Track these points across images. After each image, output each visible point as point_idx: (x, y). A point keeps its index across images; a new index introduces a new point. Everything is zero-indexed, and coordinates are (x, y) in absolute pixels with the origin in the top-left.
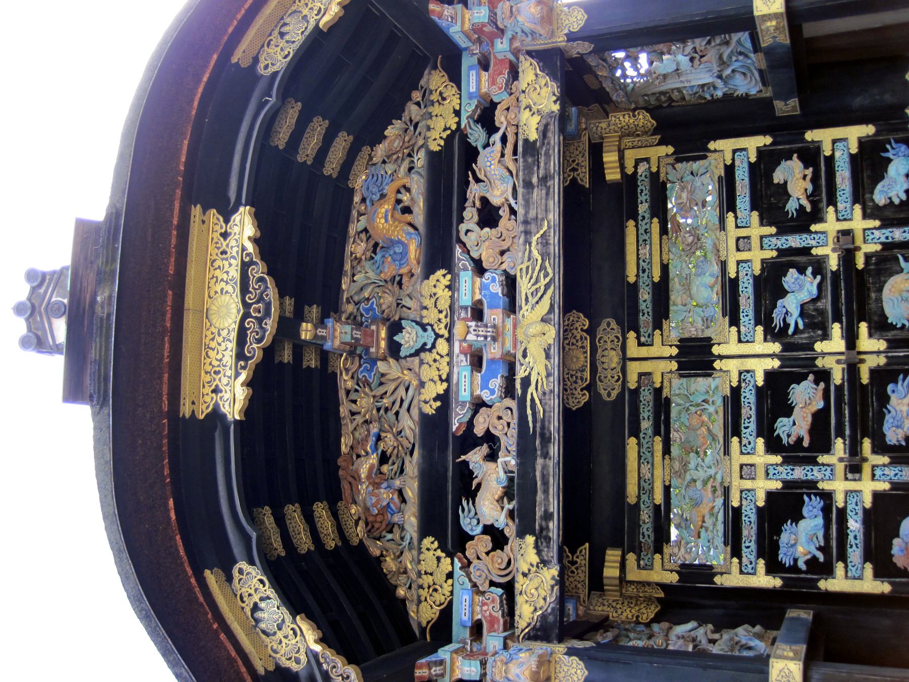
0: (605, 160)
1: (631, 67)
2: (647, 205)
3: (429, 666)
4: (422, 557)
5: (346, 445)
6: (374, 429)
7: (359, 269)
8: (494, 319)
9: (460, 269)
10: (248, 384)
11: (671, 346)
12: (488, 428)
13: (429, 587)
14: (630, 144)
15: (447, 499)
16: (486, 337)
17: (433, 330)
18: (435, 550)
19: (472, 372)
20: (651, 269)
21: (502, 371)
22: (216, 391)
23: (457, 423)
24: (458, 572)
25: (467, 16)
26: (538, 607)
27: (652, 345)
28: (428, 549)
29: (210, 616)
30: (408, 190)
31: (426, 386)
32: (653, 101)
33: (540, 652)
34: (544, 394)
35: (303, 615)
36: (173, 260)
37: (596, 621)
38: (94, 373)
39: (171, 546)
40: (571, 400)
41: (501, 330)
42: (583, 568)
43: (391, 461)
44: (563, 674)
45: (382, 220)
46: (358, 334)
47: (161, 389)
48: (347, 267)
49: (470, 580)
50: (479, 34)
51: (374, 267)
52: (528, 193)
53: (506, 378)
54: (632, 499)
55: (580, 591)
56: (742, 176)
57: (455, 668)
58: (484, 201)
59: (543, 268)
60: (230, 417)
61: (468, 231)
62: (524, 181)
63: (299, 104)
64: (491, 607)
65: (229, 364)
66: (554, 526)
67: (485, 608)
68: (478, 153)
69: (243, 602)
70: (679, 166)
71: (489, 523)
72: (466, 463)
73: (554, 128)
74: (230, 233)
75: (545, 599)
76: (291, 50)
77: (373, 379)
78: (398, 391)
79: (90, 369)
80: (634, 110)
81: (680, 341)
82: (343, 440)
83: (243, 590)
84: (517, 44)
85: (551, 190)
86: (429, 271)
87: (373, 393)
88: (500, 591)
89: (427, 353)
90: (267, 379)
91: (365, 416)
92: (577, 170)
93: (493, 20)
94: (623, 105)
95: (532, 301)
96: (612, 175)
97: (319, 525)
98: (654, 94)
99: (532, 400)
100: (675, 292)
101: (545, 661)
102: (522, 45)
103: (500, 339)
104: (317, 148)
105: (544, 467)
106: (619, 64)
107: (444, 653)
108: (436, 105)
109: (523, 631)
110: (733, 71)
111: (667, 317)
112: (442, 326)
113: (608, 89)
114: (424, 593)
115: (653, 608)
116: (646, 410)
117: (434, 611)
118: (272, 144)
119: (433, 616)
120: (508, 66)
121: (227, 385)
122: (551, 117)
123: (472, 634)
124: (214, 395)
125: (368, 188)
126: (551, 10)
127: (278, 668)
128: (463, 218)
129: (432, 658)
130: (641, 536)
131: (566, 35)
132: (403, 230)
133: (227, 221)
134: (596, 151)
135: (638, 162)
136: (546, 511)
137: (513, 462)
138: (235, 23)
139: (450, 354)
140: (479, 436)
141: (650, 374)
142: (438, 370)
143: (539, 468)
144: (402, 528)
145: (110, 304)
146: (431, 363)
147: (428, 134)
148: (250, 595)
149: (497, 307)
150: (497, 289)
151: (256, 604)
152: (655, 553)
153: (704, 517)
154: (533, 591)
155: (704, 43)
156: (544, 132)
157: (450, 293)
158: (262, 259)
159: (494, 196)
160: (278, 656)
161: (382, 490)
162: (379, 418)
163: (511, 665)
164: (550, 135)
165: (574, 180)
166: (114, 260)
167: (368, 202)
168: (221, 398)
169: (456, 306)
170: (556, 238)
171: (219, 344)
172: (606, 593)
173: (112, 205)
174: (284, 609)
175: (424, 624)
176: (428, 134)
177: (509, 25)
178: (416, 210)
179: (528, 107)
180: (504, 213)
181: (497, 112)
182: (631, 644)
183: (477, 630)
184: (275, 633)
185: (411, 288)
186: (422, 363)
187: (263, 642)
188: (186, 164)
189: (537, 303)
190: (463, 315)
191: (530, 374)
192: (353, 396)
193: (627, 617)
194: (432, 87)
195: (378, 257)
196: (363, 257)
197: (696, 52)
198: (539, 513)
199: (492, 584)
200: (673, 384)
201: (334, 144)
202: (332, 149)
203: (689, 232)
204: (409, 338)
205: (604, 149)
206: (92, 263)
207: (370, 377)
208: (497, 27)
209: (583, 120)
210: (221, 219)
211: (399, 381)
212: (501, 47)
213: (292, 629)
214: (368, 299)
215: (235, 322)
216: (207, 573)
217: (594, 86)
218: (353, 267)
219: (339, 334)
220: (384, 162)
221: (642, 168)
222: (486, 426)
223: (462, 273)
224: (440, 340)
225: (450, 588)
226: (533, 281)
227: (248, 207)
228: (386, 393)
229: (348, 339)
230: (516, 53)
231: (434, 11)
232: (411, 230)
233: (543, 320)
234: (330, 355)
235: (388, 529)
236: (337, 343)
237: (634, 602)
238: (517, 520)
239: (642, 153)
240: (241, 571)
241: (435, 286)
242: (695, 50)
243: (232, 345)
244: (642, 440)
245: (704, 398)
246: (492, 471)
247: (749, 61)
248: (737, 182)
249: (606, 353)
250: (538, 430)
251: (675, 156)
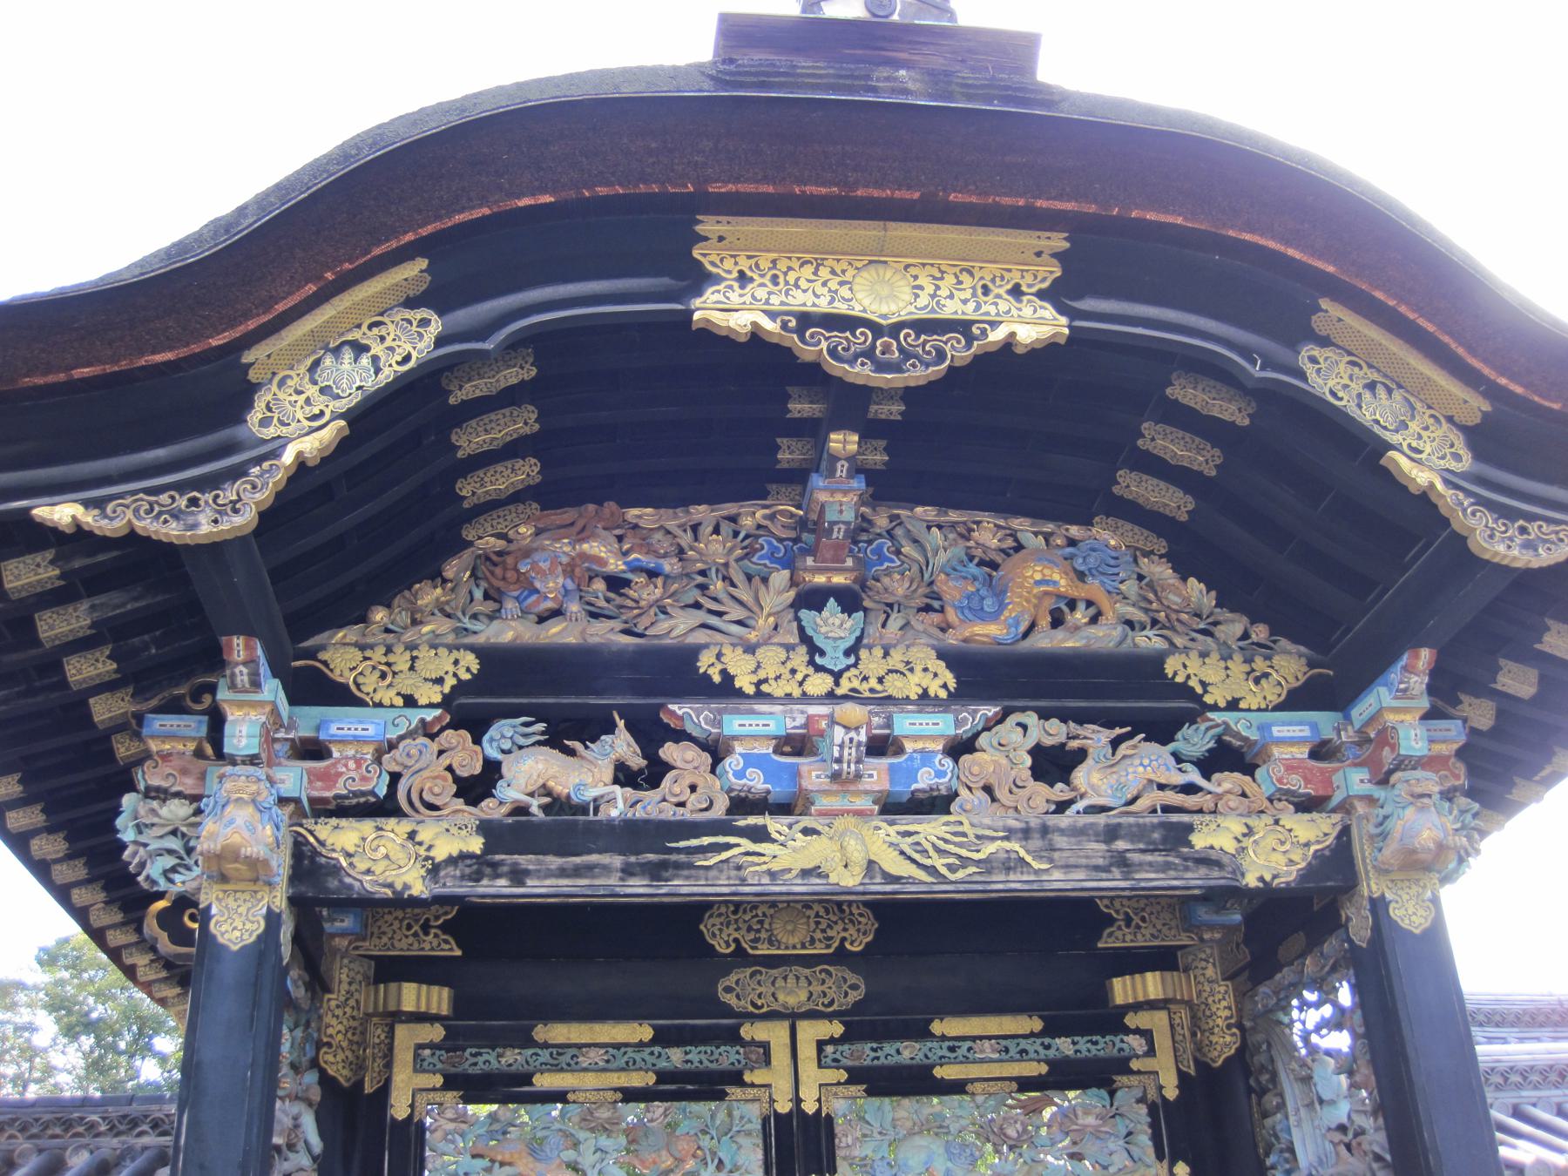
0: (1149, 975)
1: (1323, 1018)
2: (1071, 1053)
3: (251, 662)
4: (443, 651)
5: (640, 517)
6: (669, 566)
7: (951, 536)
8: (871, 776)
9: (956, 714)
10: (756, 336)
11: (819, 1100)
12: (674, 768)
13: (389, 664)
14: (1178, 1021)
15: (547, 695)
16: (839, 761)
17: (848, 668)
18: (455, 675)
19: (775, 738)
20: (956, 1061)
21: (778, 792)
22: (743, 279)
23: (684, 711)
24: (416, 716)
25: (1408, 717)
26: (355, 860)
27: (820, 1066)
28: (456, 662)
29: (347, 266)
30: (1094, 620)
31: (748, 657)
32: (1261, 1059)
33: (274, 864)
34: (739, 868)
35: (347, 432)
36: (974, 199)
37: (323, 968)
38: (774, 65)
39: (470, 199)
40: (717, 921)
41: (852, 788)
42: (416, 946)
43: (612, 595)
44: (232, 904)
45: (1039, 577)
46: (838, 533)
47: (747, 181)
48: (954, 516)
49: (402, 738)
50: (1375, 740)
51: (954, 563)
52: (1097, 835)
53: (765, 799)
54: (541, 1032)
55: (375, 941)
57: (246, 710)
58: (1081, 755)
59: (965, 862)
60: (697, 302)
61: (1024, 727)
62: (1119, 825)
63: (1247, 422)
64: (354, 774)
65: (790, 300)
66: (502, 886)
67: (352, 765)
68: (1164, 743)
69: (370, 327)
70: (1143, 1110)
71: (504, 770)
72: (610, 728)
73: (1216, 878)
74: (1019, 301)
75: (368, 872)
76: (1346, 403)
77: (757, 563)
78: (737, 606)
79: (781, 60)
80: (1240, 1026)
81: (828, 1115)
82: (649, 510)
83: (391, 327)
84: (1361, 808)
85: (1104, 875)
86: (952, 659)
87: (733, 563)
88: (382, 791)
89: (807, 658)
90: (763, 364)
91: (692, 548)
92: (1128, 926)
93: (1402, 764)
94: (1248, 1006)
95: (905, 844)
96: (1122, 990)
97: (499, 468)
98: (1272, 1061)
99: (728, 847)
100: (916, 1106)
101: (257, 872)
102: (1360, 818)
103: (835, 787)
104: (1167, 457)
105: (607, 869)
106: (1328, 995)
107: (272, 689)
108: (1246, 668)
109: (311, 833)
111: (870, 1093)
112: (856, 684)
113: (1278, 976)
114: (378, 655)
115: (345, 1072)
116: (703, 1057)
117: (347, 673)
118: (1174, 375)
119: (337, 672)
120: (1321, 793)
121: (753, 297)
122: (1234, 872)
123: (304, 741)
124: (735, 275)
125: (1094, 550)
126: (1427, 868)
127: (254, 388)
128: (1047, 719)
129: (264, 669)
130: (474, 1050)
131: (1383, 896)
132: (1022, 613)
133: (1041, 295)
134: (1163, 960)
135: (1147, 1034)
136: (527, 873)
137: (614, 813)
138: (1392, 303)
139: (806, 698)
140: (661, 752)
141: (768, 1062)
142: (778, 678)
143: (605, 859)
144: (492, 617)
145: (893, 91)
146: (789, 665)
147: (1194, 655)
148: (382, 339)
149: (892, 781)
150: (925, 780)
151: (366, 349)
152: (445, 1076)
153: (510, 1164)
154: (383, 850)
155: (1377, 1149)
156: (1206, 860)
157: (914, 697)
158: (976, 357)
159: (1089, 774)
160: (274, 388)
161: (564, 579)
162: (687, 575)
163: (251, 809)
164: (1203, 871)
165: (1110, 921)
166: (970, 98)
167: (1070, 550)
168: (731, 287)
169: (892, 708)
170: (1018, 886)
171: (824, 284)
172: (372, 988)
173: (1065, 96)
174: (357, 398)
175: (323, 656)
176: (1194, 655)
177: (1396, 792)
178: (1059, 634)
179: (1250, 832)
180: (1060, 791)
181: (1237, 775)
182: (285, 1031)
183: (312, 750)
184: (315, 383)
185: (920, 627)
186: (789, 648)
187: (299, 361)
188: (1141, 222)
189: (902, 853)
190: (876, 720)
191: (774, 841)
192: (726, 528)
193: (328, 1026)
194: (1276, 660)
195: (972, 568)
196: (972, 543)
197: (1356, 1135)
198: (525, 861)
199: (395, 778)
200: (749, 1106)
201: (1172, 488)
202: (1162, 484)
203: (1025, 1130)
204: (832, 625)
205: (1168, 974)
206: (963, 61)
207: (761, 558)
208: (1391, 772)
209: (1217, 936)
210: (1045, 285)
211: (755, 609)
212: (1355, 781)
213: (322, 413)
214: (898, 552)
215: (865, 311)
216: (423, 263)
217: (1283, 952)
218: (953, 525)
219: (838, 500)
220: (1140, 577)
221: (1136, 1043)
222: (679, 764)
223: (950, 717)
224: (829, 680)
225: (386, 702)
226: (941, 844)
227: (1066, 331)
228: (733, 585)
229: (831, 516)
230: (1345, 807)
231: (1417, 657)
232: (1022, 628)
233: (871, 863)
234: (799, 488)
235: (492, 592)
236: (823, 497)
237: (355, 1038)
238: (510, 820)
239: (1163, 1042)
240: (424, 323)
241: (926, 670)
242: (1360, 1132)
243: (823, 306)
244: (648, 1050)
245: (727, 1162)
246: (597, 776)
249: (803, 983)
250: (674, 857)
251: (1159, 1101)
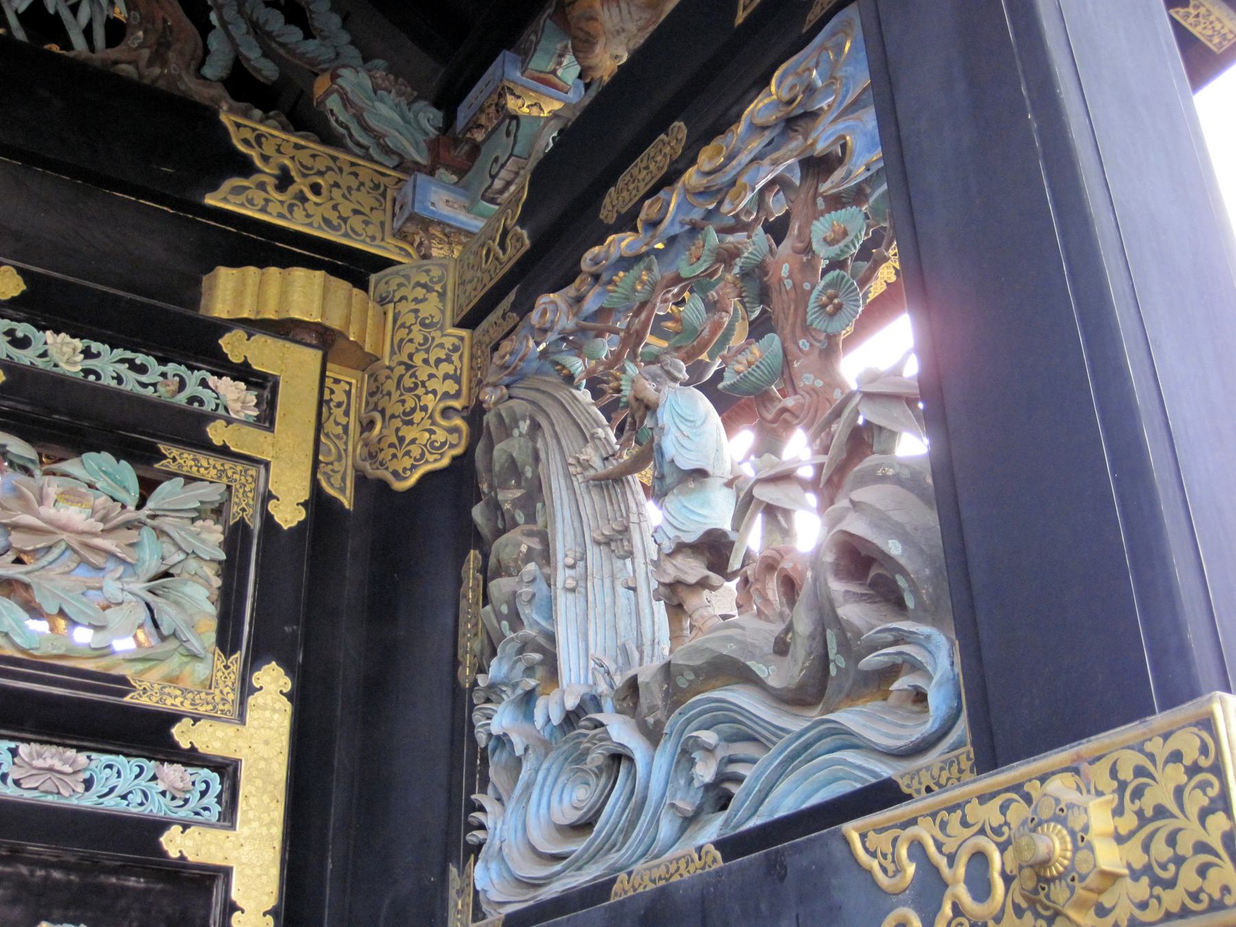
14: (339, 396)
56: (112, 783)
70: (212, 536)
80: (475, 414)
96: (229, 292)
98: (537, 458)
110: (618, 758)
135: (262, 384)
165: (244, 167)
221: (231, 391)
247: (666, 828)
248: (82, 758)
251: (256, 525)
